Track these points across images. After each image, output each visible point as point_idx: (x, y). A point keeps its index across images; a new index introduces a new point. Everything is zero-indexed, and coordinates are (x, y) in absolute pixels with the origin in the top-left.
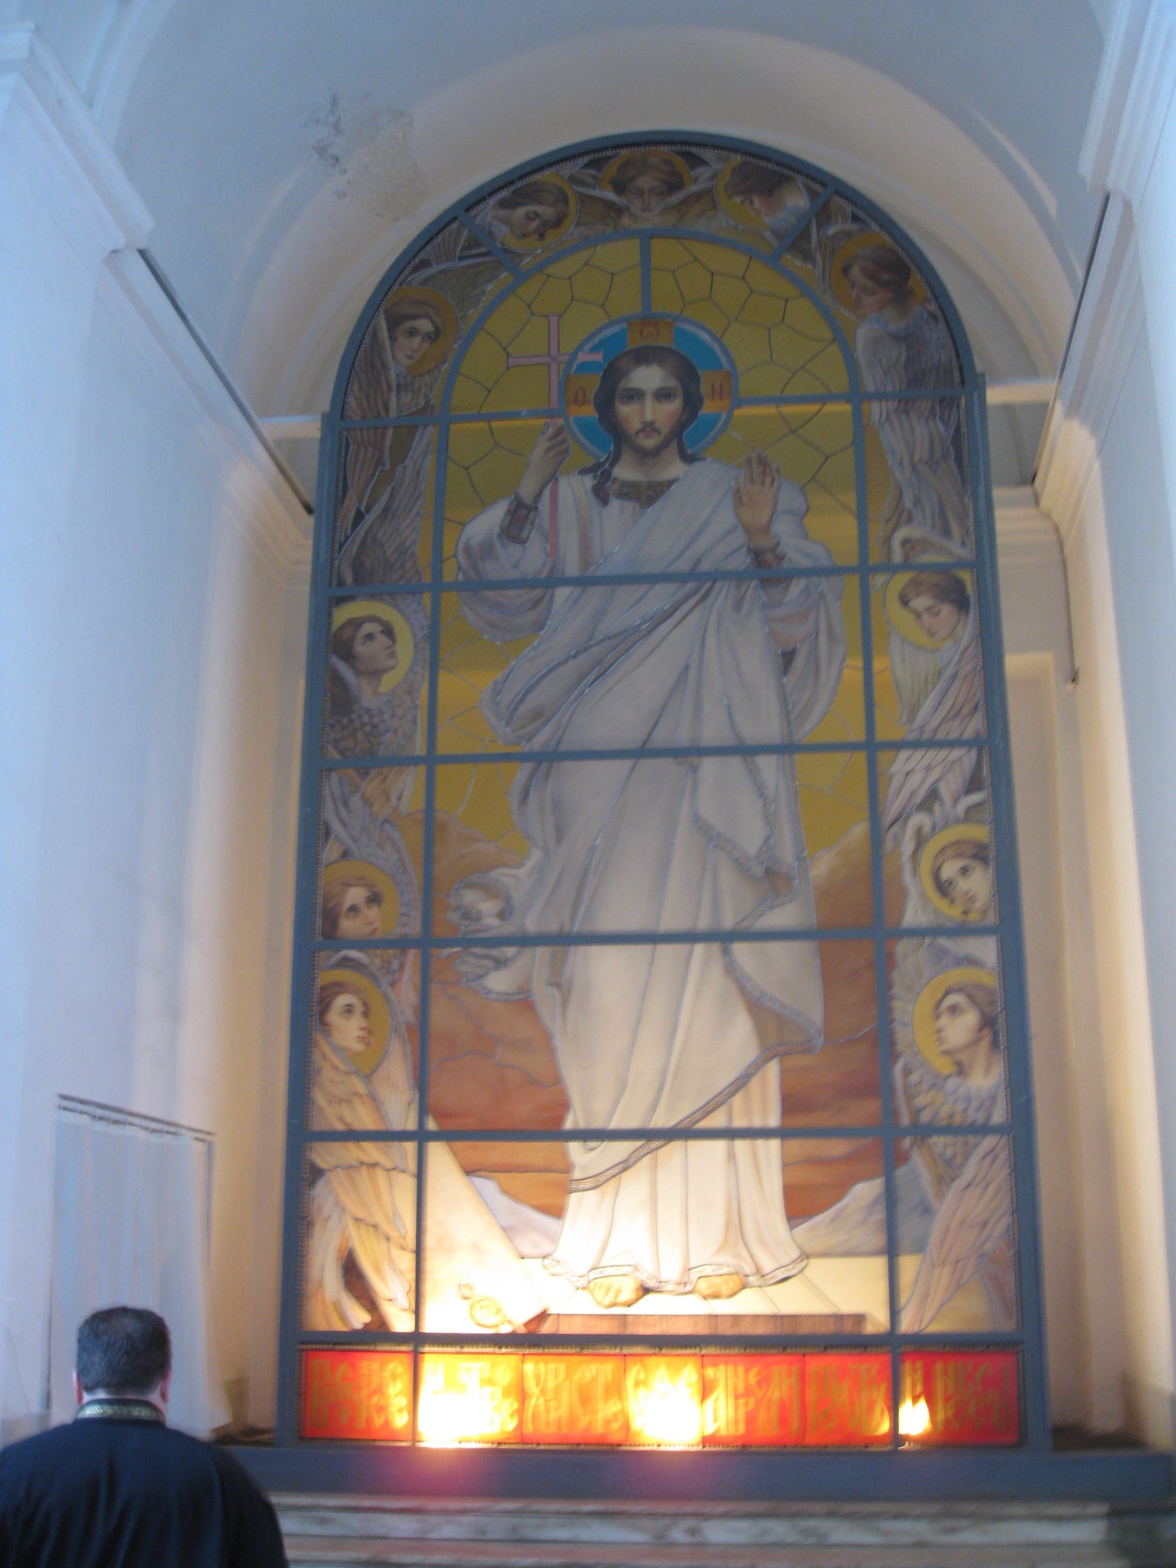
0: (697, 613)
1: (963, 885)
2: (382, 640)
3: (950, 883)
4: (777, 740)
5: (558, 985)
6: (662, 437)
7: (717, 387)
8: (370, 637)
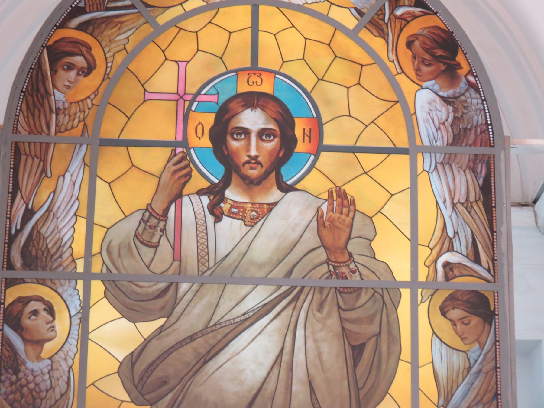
2: (44, 314)
6: (263, 170)
7: (307, 132)
8: (35, 313)
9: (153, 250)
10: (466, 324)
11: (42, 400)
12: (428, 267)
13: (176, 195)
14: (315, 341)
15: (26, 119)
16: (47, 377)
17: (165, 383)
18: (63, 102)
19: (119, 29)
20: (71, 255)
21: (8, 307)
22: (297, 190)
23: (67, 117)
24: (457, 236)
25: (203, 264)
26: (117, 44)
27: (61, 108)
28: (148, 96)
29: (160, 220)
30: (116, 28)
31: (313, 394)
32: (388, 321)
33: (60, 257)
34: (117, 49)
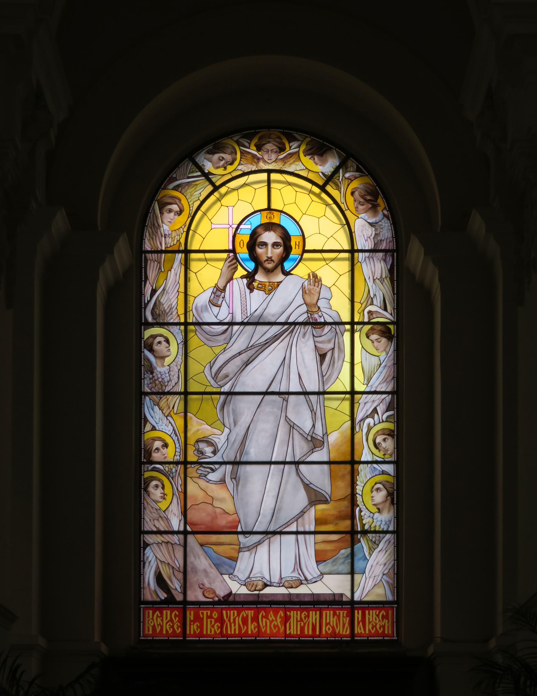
0: (288, 338)
1: (384, 445)
2: (164, 344)
3: (379, 443)
4: (317, 390)
5: (235, 478)
6: (275, 264)
7: (297, 243)
8: (160, 343)
9: (219, 308)
10: (379, 342)
11: (166, 386)
12: (360, 313)
13: (230, 279)
14: (301, 353)
15: (149, 241)
16: (168, 375)
17: (227, 376)
18: (168, 231)
19: (195, 188)
20: (177, 313)
21: (146, 340)
22: (292, 274)
23: (171, 239)
24: (375, 296)
25: (244, 315)
26: (194, 197)
27: (167, 234)
28: (213, 226)
29: (222, 292)
30: (194, 188)
31: (300, 379)
32: (338, 342)
33: (171, 314)
34: (195, 200)
